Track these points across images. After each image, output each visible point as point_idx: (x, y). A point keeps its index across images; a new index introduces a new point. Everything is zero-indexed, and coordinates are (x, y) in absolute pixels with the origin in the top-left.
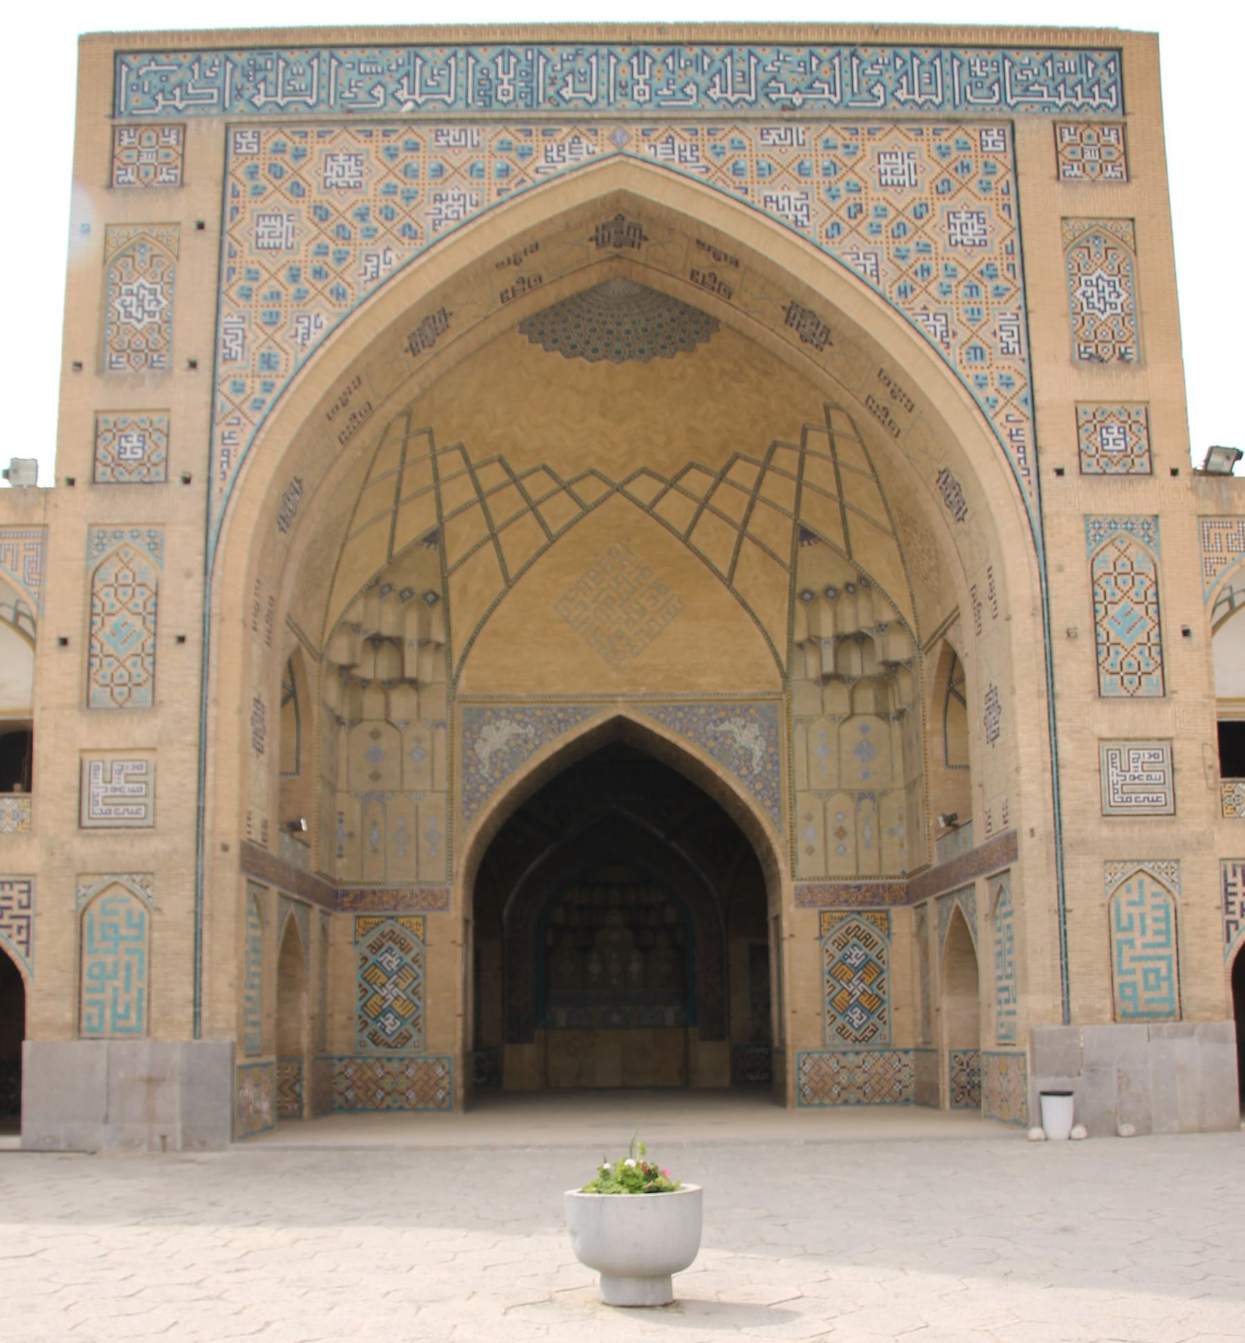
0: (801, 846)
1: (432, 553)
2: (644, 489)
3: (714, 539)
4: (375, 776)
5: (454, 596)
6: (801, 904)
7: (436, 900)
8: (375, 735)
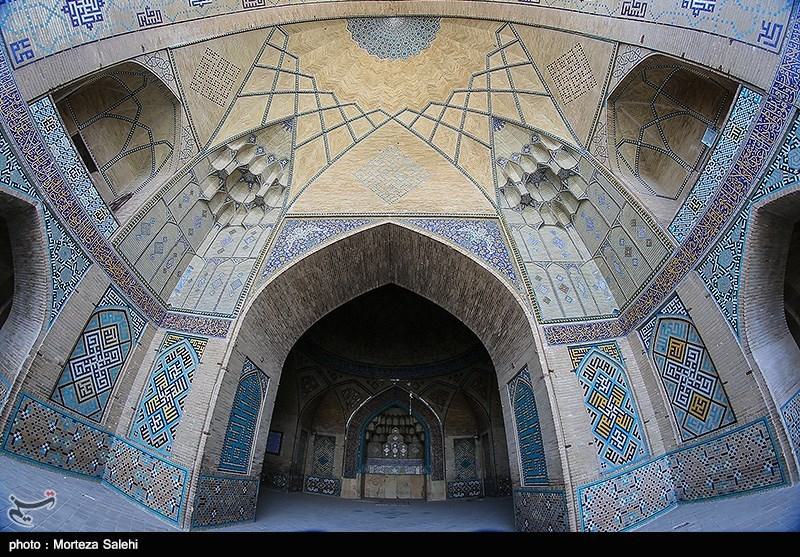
0: (539, 298)
1: (288, 135)
2: (407, 118)
3: (446, 140)
4: (222, 251)
5: (296, 161)
6: (552, 343)
7: (219, 328)
8: (232, 232)
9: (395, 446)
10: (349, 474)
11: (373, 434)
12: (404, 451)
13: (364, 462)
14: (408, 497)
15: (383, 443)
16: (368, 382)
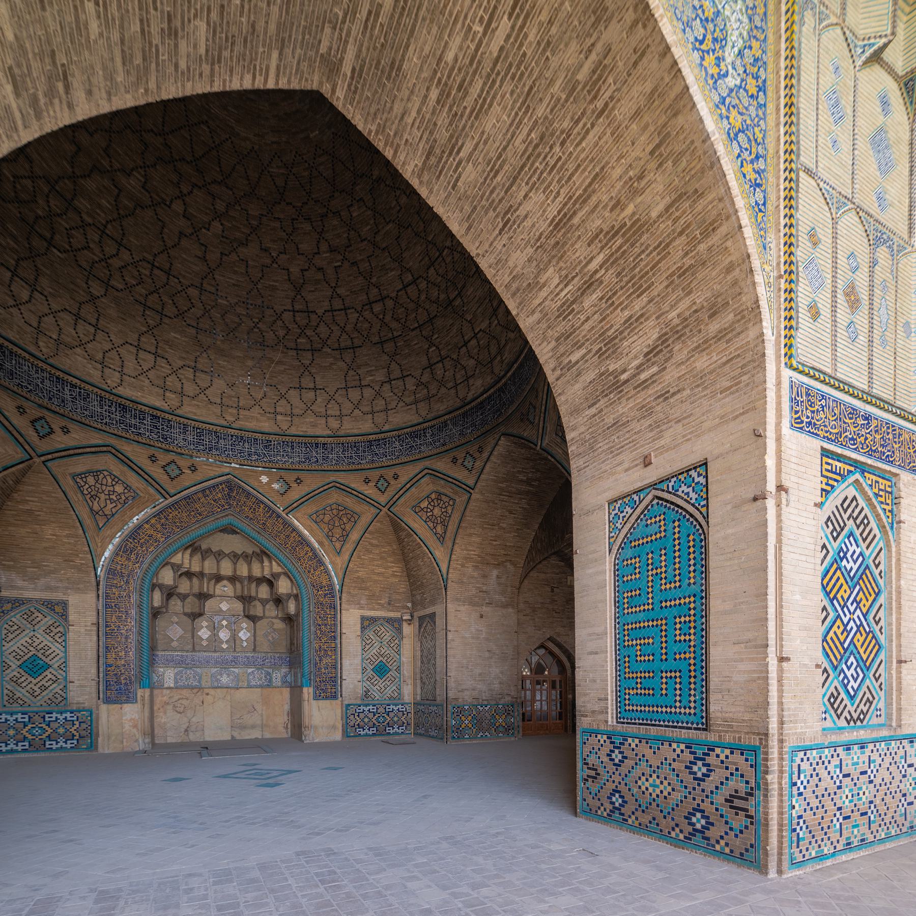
9: (224, 623)
10: (115, 689)
11: (170, 593)
12: (244, 635)
13: (152, 662)
14: (256, 734)
15: (196, 616)
16: (153, 459)
